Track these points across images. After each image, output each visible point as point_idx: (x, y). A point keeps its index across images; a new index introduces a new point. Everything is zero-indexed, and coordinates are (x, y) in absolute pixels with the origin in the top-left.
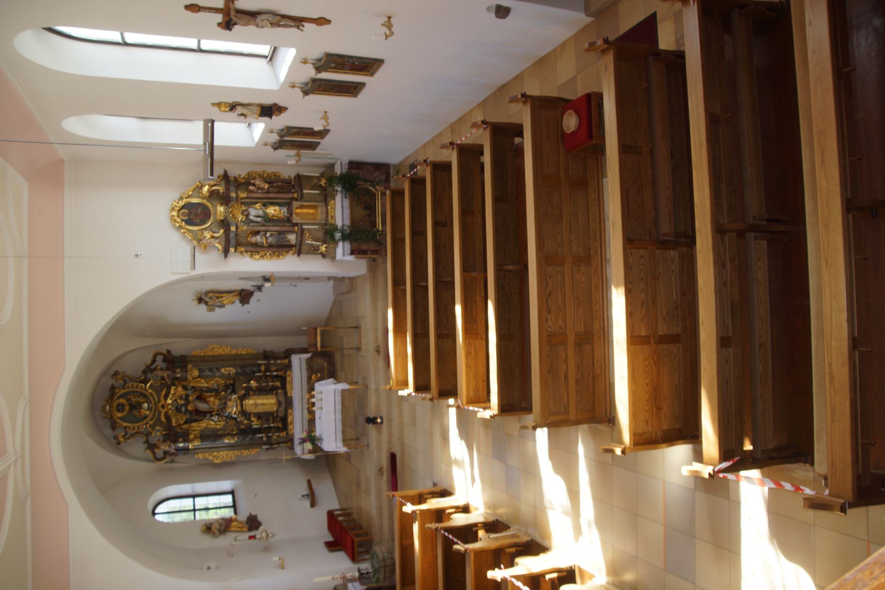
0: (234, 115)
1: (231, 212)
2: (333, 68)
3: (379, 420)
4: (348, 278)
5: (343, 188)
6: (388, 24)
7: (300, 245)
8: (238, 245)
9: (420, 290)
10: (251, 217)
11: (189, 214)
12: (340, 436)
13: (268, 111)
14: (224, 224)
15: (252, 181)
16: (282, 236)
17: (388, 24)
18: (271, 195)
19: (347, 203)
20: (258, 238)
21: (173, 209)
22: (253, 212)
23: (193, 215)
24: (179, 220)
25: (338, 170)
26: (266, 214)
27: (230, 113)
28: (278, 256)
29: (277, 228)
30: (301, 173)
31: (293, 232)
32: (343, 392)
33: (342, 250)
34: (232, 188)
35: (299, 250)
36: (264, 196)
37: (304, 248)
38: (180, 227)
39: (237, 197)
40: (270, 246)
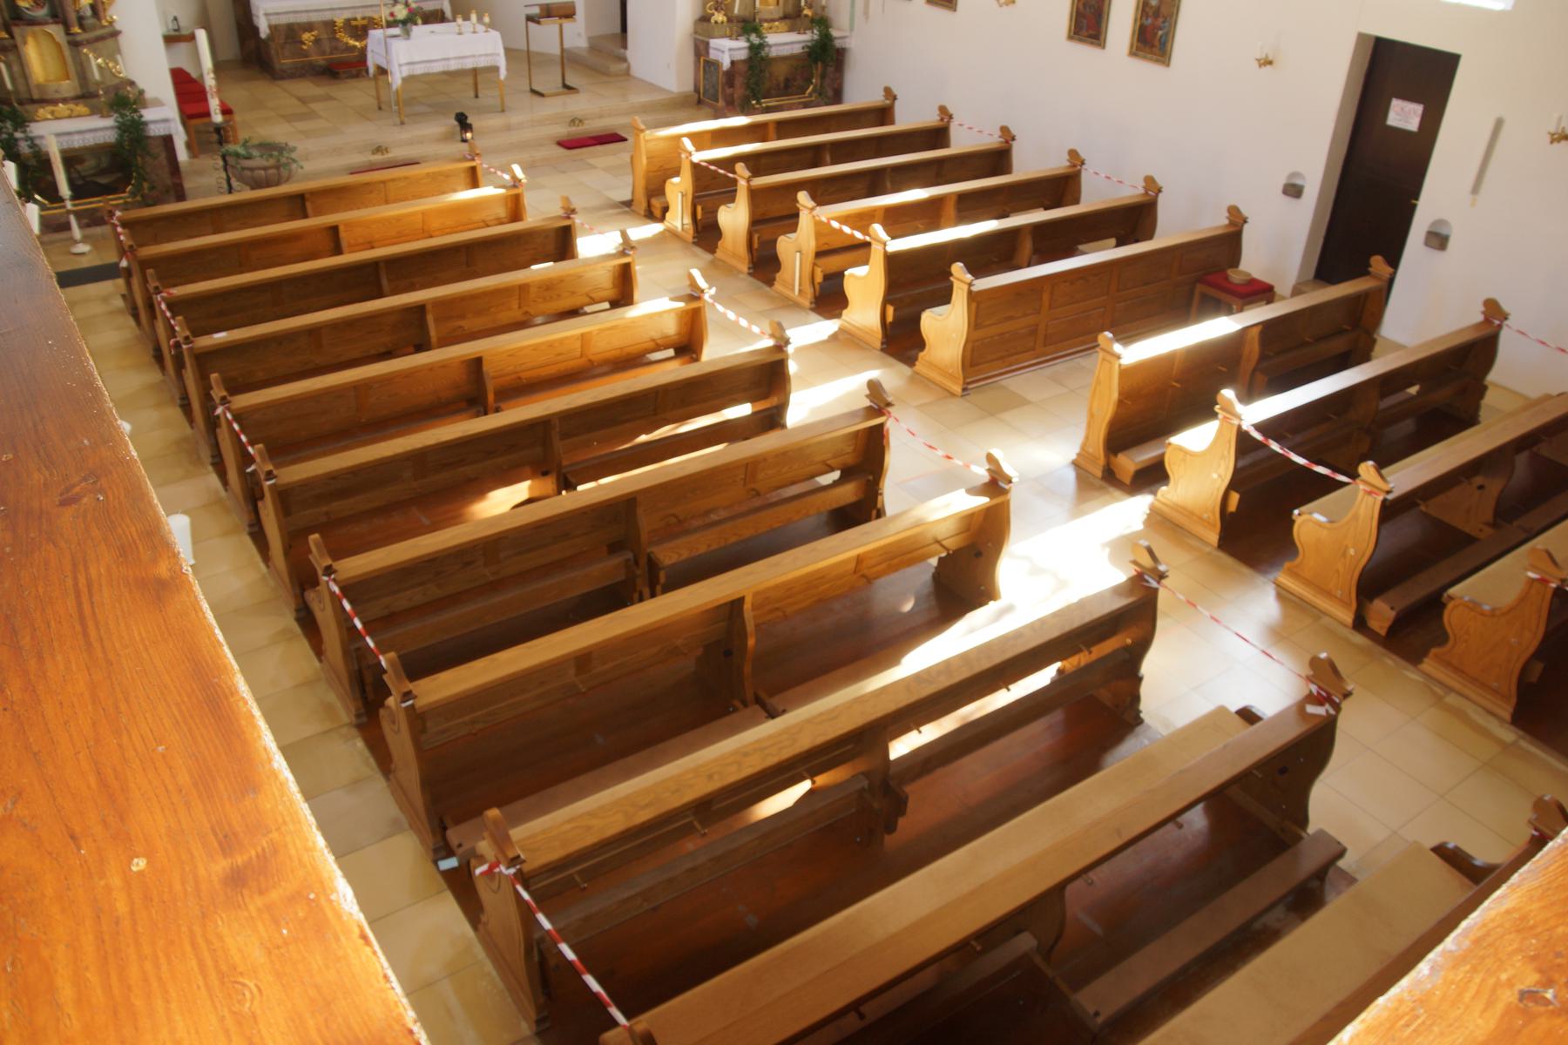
3: (469, 135)
4: (628, 68)
9: (814, 155)
12: (419, 70)
19: (797, 49)
25: (834, 33)
32: (495, 69)
33: (728, 50)
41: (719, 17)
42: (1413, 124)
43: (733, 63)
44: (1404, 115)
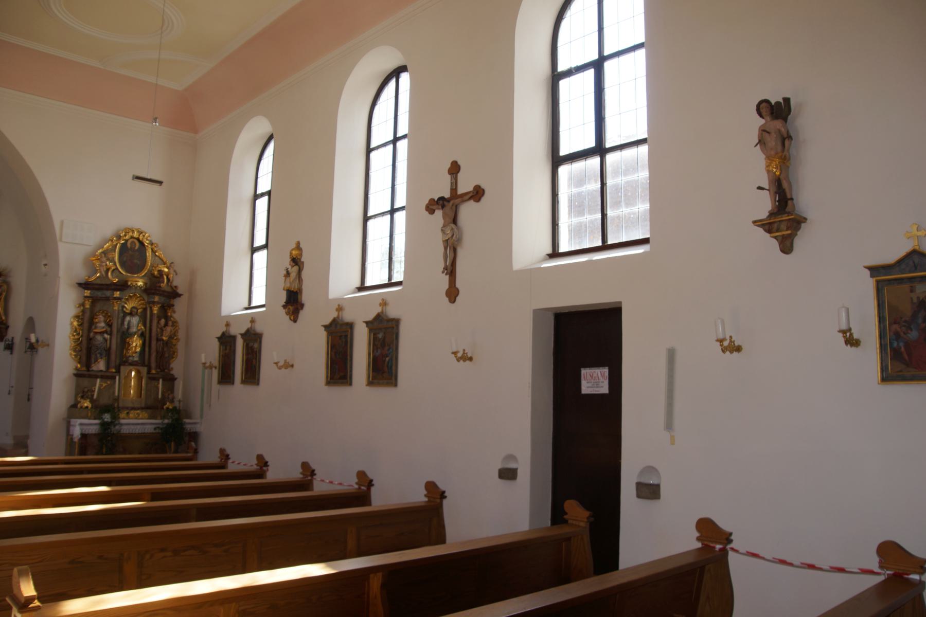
0: (287, 262)
1: (135, 295)
2: (375, 339)
5: (167, 424)
6: (466, 358)
7: (90, 376)
8: (94, 300)
10: (128, 318)
11: (132, 249)
13: (293, 302)
14: (123, 286)
15: (170, 323)
16: (104, 354)
17: (466, 358)
18: (154, 343)
19: (149, 429)
20: (101, 325)
21: (140, 233)
22: (135, 320)
23: (132, 251)
24: (127, 237)
26: (132, 335)
27: (288, 260)
28: (75, 351)
29: (114, 347)
30: (176, 382)
31: (108, 367)
34: (163, 299)
35: (84, 374)
36: (154, 334)
37: (86, 382)
38: (119, 237)
39: (154, 303)
40: (90, 340)
41: (87, 404)
42: (604, 389)
43: (84, 436)
44: (594, 381)
